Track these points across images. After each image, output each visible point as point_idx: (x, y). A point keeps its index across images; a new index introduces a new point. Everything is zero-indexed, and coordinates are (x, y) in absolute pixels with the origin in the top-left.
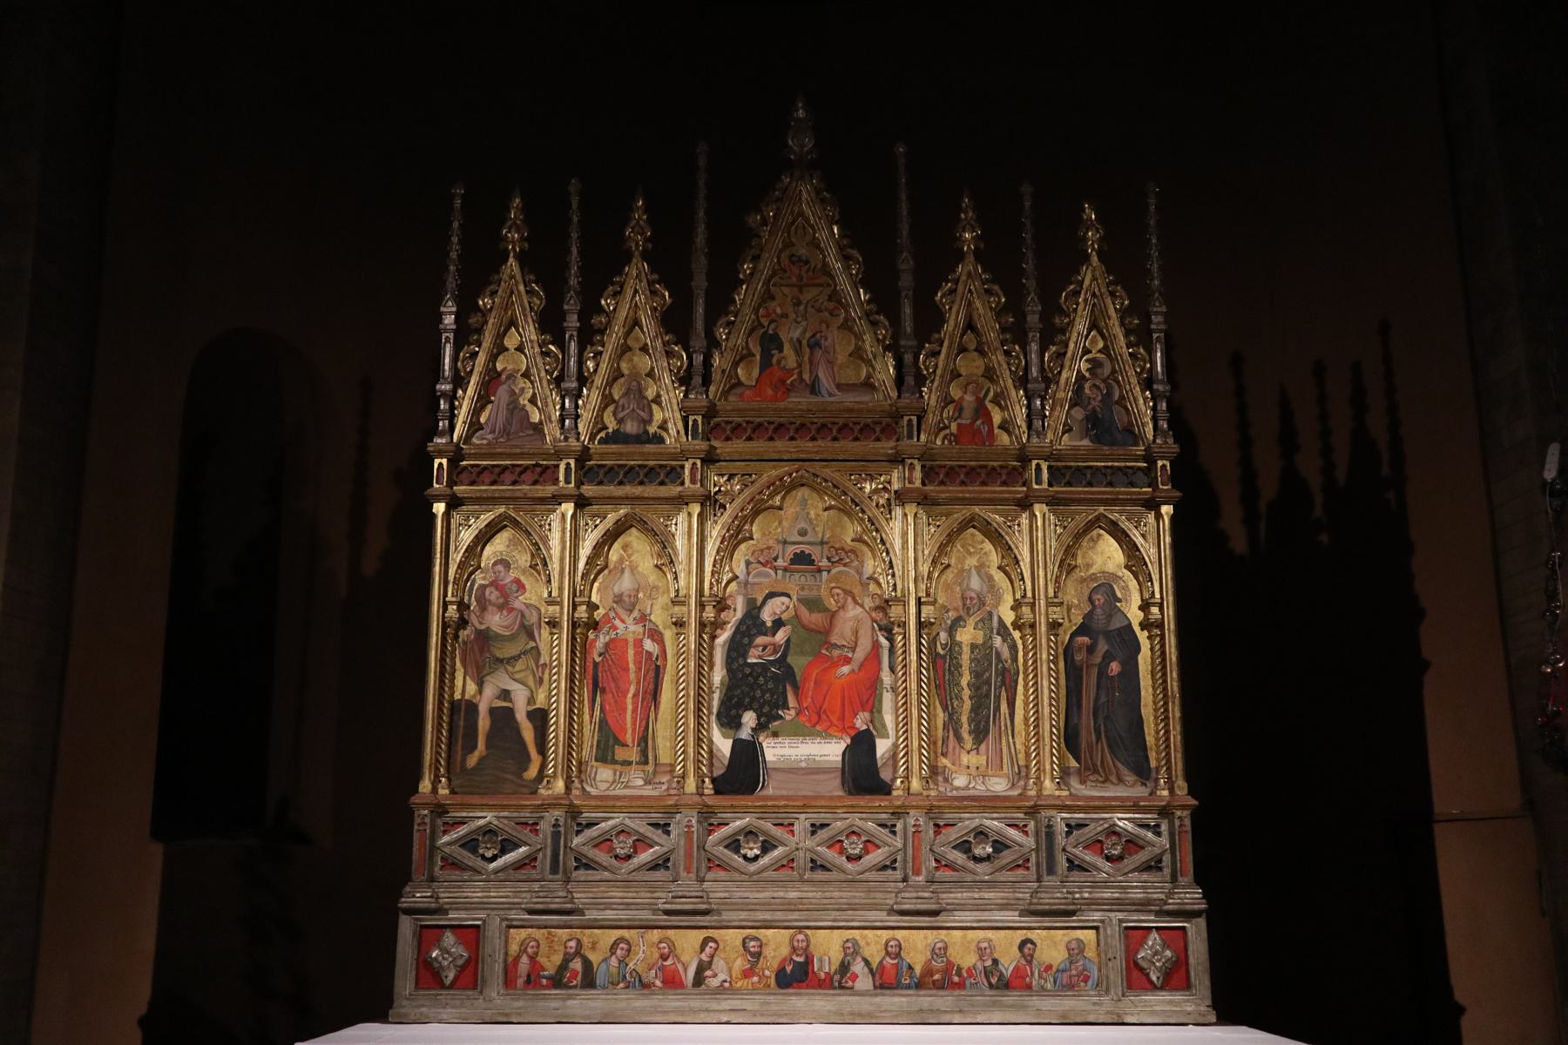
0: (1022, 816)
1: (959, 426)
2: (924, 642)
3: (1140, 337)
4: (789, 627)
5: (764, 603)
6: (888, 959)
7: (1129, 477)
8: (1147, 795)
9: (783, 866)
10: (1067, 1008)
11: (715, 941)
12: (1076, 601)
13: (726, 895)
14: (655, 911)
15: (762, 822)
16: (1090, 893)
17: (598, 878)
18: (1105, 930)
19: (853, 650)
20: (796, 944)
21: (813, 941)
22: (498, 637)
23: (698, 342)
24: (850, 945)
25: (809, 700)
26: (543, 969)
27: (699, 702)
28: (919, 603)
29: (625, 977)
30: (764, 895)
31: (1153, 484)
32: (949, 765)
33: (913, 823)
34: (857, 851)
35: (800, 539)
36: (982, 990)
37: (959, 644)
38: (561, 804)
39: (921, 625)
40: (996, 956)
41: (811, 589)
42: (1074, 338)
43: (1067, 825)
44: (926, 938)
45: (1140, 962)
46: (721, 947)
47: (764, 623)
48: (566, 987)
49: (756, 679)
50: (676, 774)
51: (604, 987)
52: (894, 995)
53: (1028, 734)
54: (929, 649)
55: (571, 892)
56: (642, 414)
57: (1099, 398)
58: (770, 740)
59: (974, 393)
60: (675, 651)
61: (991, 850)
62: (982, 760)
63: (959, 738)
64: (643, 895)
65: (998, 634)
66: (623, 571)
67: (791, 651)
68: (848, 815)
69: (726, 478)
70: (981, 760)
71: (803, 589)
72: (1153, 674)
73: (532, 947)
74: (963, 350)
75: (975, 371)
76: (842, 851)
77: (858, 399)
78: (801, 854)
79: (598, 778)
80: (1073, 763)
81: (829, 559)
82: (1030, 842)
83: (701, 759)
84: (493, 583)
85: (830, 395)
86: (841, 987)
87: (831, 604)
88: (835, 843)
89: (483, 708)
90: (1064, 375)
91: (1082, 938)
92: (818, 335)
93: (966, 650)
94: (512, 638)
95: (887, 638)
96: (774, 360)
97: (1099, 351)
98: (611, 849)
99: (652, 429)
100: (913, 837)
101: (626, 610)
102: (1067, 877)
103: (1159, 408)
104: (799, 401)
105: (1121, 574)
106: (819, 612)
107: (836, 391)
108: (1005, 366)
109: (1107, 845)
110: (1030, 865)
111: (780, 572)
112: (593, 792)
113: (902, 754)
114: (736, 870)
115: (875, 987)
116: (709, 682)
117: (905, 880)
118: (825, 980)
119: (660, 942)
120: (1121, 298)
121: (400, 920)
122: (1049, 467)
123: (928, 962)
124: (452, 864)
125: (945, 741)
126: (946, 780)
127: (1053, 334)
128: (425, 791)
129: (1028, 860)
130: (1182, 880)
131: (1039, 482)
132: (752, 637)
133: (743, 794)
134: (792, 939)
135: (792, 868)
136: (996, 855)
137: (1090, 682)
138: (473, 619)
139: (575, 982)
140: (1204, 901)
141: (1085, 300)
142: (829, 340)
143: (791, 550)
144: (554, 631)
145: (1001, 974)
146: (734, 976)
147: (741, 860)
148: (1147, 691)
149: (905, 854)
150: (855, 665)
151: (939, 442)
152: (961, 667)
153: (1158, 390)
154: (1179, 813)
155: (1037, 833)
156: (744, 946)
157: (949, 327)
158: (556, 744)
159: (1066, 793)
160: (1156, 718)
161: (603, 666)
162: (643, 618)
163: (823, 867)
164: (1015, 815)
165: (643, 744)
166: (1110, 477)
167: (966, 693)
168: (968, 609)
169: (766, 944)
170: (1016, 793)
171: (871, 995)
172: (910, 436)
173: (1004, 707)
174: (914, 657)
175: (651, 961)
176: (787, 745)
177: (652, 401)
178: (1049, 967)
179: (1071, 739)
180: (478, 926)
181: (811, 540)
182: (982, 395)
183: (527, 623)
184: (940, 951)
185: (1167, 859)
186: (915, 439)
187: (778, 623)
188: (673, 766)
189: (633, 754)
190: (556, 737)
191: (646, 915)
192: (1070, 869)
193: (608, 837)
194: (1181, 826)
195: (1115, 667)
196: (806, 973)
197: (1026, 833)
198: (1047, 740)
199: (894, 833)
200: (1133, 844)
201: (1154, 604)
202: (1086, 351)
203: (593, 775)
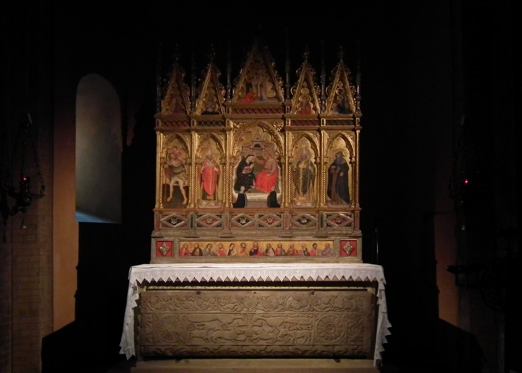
0: (315, 213)
1: (301, 109)
2: (290, 168)
3: (353, 82)
6: (279, 249)
7: (348, 122)
12: (332, 156)
13: (236, 233)
14: (218, 237)
15: (246, 215)
17: (203, 229)
18: (335, 241)
19: (271, 170)
20: (255, 245)
22: (175, 167)
23: (229, 86)
26: (189, 251)
28: (289, 157)
29: (210, 253)
30: (247, 232)
32: (296, 200)
34: (271, 222)
35: (257, 140)
39: (290, 164)
40: (307, 248)
43: (327, 215)
45: (344, 249)
47: (247, 163)
49: (245, 178)
50: (223, 203)
51: (205, 256)
53: (317, 192)
56: (213, 106)
57: (341, 100)
58: (248, 194)
59: (306, 100)
62: (305, 198)
63: (299, 193)
65: (310, 165)
66: (208, 149)
67: (254, 170)
68: (269, 213)
70: (305, 198)
71: (257, 154)
72: (352, 175)
74: (303, 87)
76: (267, 222)
78: (256, 223)
79: (202, 204)
80: (329, 199)
81: (265, 146)
82: (317, 219)
84: (173, 153)
85: (266, 100)
86: (266, 255)
87: (265, 158)
89: (171, 186)
90: (332, 94)
93: (301, 170)
94: (178, 167)
95: (280, 167)
96: (250, 90)
97: (342, 87)
98: (206, 222)
99: (216, 110)
104: (258, 102)
105: (345, 149)
107: (267, 99)
110: (316, 225)
111: (251, 149)
112: (201, 207)
114: (239, 227)
115: (275, 255)
116: (232, 178)
117: (283, 229)
119: (219, 245)
122: (326, 120)
123: (289, 249)
124: (165, 225)
125: (295, 194)
126: (295, 204)
127: (329, 83)
129: (316, 224)
130: (356, 229)
131: (323, 124)
132: (244, 167)
135: (254, 226)
137: (335, 178)
138: (168, 162)
141: (338, 73)
143: (255, 143)
146: (238, 252)
147: (240, 224)
149: (284, 222)
151: (295, 113)
152: (300, 174)
154: (356, 212)
155: (319, 217)
157: (299, 81)
158: (191, 195)
159: (327, 207)
162: (214, 162)
163: (262, 226)
166: (342, 122)
167: (301, 181)
168: (302, 159)
170: (313, 207)
172: (288, 112)
173: (311, 185)
174: (287, 172)
179: (329, 193)
180: (172, 241)
181: (260, 140)
183: (182, 164)
185: (353, 223)
186: (289, 113)
187: (251, 163)
188: (222, 201)
189: (212, 198)
190: (191, 193)
191: (216, 238)
193: (205, 219)
195: (342, 174)
196: (257, 252)
197: (316, 217)
199: (281, 217)
200: (344, 219)
201: (353, 157)
202: (338, 87)
203: (201, 203)
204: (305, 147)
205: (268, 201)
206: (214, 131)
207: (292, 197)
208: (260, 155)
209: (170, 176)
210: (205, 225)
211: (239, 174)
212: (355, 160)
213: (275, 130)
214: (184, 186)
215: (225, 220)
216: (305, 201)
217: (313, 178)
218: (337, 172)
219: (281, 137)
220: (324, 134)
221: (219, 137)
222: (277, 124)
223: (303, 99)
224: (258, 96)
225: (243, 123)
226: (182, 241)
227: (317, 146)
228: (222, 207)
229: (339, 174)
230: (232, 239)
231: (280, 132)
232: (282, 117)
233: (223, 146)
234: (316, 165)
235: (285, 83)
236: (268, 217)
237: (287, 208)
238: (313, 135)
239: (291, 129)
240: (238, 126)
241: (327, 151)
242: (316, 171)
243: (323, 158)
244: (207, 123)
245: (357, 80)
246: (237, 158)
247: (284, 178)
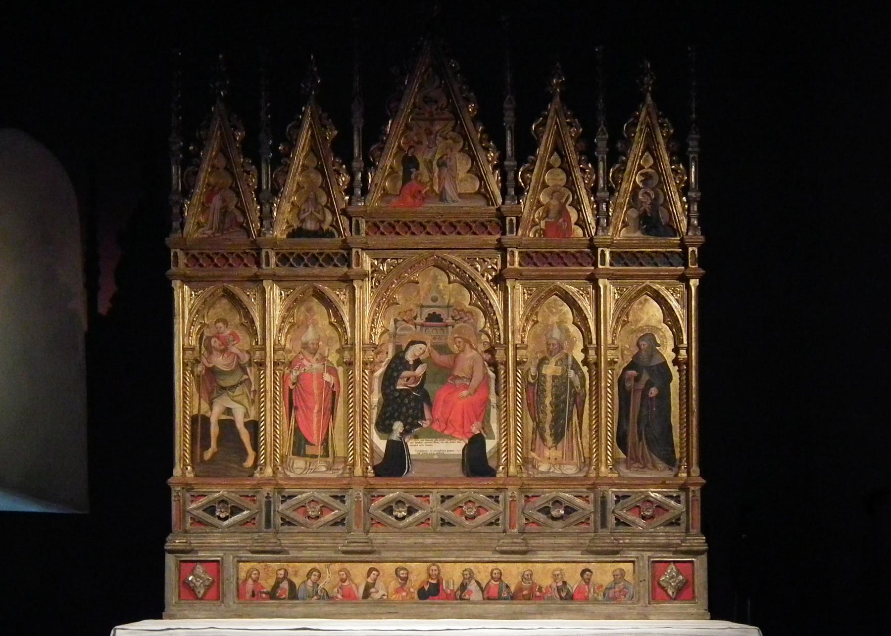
0: (585, 490)
3: (680, 156)
4: (424, 364)
5: (407, 348)
6: (493, 582)
7: (667, 258)
8: (672, 476)
9: (422, 523)
10: (611, 611)
11: (377, 570)
12: (628, 346)
13: (384, 541)
14: (336, 552)
15: (407, 494)
16: (630, 540)
18: (639, 563)
19: (470, 380)
20: (431, 572)
21: (442, 570)
22: (222, 373)
23: (357, 164)
24: (467, 572)
25: (439, 414)
26: (263, 588)
27: (363, 415)
28: (516, 348)
29: (317, 592)
30: (411, 541)
31: (686, 265)
32: (536, 457)
33: (510, 495)
37: (544, 376)
38: (270, 484)
39: (518, 364)
40: (565, 579)
41: (440, 338)
42: (631, 158)
43: (616, 496)
44: (518, 568)
45: (661, 582)
46: (381, 574)
47: (408, 362)
48: (279, 599)
49: (402, 401)
50: (348, 463)
51: (303, 599)
52: (496, 604)
53: (591, 436)
54: (523, 379)
55: (279, 540)
56: (318, 216)
57: (649, 202)
58: (412, 441)
59: (559, 200)
60: (346, 381)
61: (563, 512)
63: (543, 439)
64: (328, 541)
66: (307, 327)
68: (466, 490)
69: (380, 260)
70: (559, 453)
71: (435, 338)
72: (680, 395)
73: (255, 574)
74: (550, 167)
75: (560, 183)
76: (463, 513)
77: (473, 205)
78: (434, 515)
79: (295, 466)
80: (623, 456)
81: (453, 318)
82: (590, 507)
83: (365, 453)
85: (454, 201)
86: (461, 599)
87: (455, 348)
88: (457, 507)
89: (213, 421)
90: (624, 185)
92: (445, 157)
93: (549, 379)
94: (232, 372)
95: (494, 372)
96: (413, 176)
97: (650, 167)
98: (306, 512)
99: (326, 227)
100: (510, 504)
101: (311, 353)
102: (614, 529)
103: (692, 209)
104: (432, 206)
105: (661, 327)
106: (447, 354)
107: (458, 198)
108: (581, 180)
109: (643, 507)
110: (590, 522)
111: (418, 327)
112: (292, 475)
113: (503, 450)
114: (390, 525)
115: (484, 599)
116: (369, 402)
117: (504, 531)
119: (340, 571)
120: (667, 127)
121: (166, 557)
122: (611, 252)
123: (519, 584)
126: (534, 467)
127: (615, 157)
128: (177, 475)
130: (693, 531)
131: (603, 263)
132: (399, 372)
133: (395, 476)
134: (428, 570)
135: (428, 524)
136: (566, 515)
138: (204, 360)
139: (284, 596)
140: (706, 544)
141: (641, 130)
142: (453, 161)
143: (426, 312)
144: (261, 368)
145: (568, 590)
146: (390, 591)
147: (393, 519)
148: (675, 407)
150: (471, 390)
151: (531, 235)
152: (545, 391)
153: (691, 196)
154: (692, 488)
155: (595, 501)
156: (396, 574)
157: (540, 151)
158: (265, 444)
159: (616, 475)
160: (681, 424)
161: (296, 392)
162: (323, 358)
163: (450, 524)
164: (580, 490)
165: (325, 444)
166: (652, 259)
167: (549, 409)
168: (551, 352)
170: (582, 475)
171: (481, 604)
173: (575, 418)
174: (511, 385)
176: (424, 444)
177: (326, 206)
178: (601, 586)
179: (621, 441)
180: (217, 561)
181: (441, 304)
182: (563, 200)
183: (241, 363)
185: (683, 518)
187: (418, 362)
188: (346, 459)
189: (319, 451)
190: (265, 439)
192: (617, 524)
193: (304, 504)
194: (693, 496)
195: (653, 391)
196: (438, 591)
197: (588, 501)
198: (603, 441)
199: (498, 502)
200: (660, 508)
201: (682, 348)
202: (641, 167)
203: (291, 465)
204: (557, 323)
205: (463, 460)
206: (322, 279)
207: (527, 449)
208: (442, 342)
209: (210, 393)
210: (301, 521)
211: (388, 391)
212: (686, 357)
213: (480, 277)
214: (246, 420)
215: (354, 507)
216: (559, 460)
217: (578, 400)
218: (641, 386)
219: (494, 297)
220: (605, 287)
221: (334, 296)
222: (485, 261)
223: (552, 199)
224: (433, 191)
225: (397, 259)
226: (244, 562)
227: (589, 320)
228: (347, 475)
229: (645, 391)
230: (371, 556)
231: (492, 284)
232: (496, 245)
233: (346, 319)
234: (585, 367)
235: (502, 157)
236: (464, 502)
237: (514, 479)
238: (578, 292)
239: (521, 275)
240: (384, 268)
241: (614, 333)
242: (588, 382)
243: (606, 350)
244: (303, 259)
245: (690, 149)
246: (383, 348)
247: (506, 401)
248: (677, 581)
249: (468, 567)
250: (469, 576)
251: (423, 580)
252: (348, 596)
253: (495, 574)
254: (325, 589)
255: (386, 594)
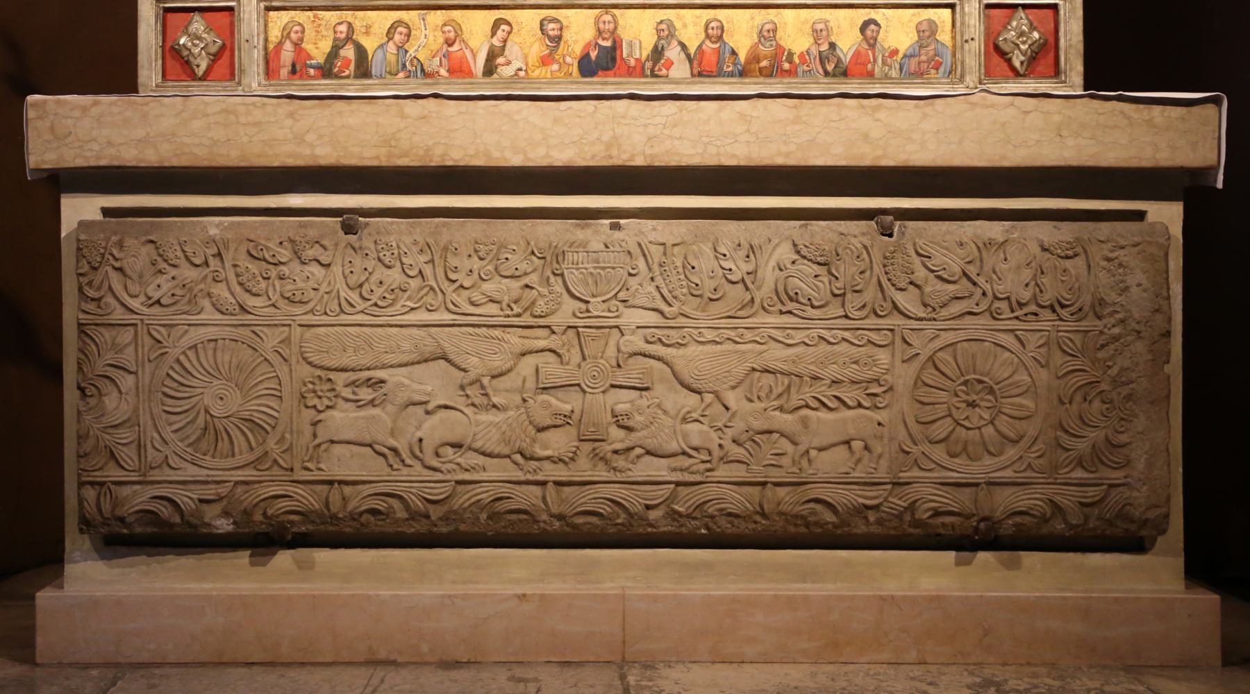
6: (708, 43)
11: (509, 24)
20: (601, 25)
21: (621, 22)
24: (664, 26)
26: (310, 58)
29: (404, 65)
36: (817, 77)
40: (833, 39)
45: (1001, 44)
46: (515, 30)
48: (337, 76)
73: (297, 32)
86: (653, 75)
91: (934, 18)
115: (693, 75)
118: (634, 68)
119: (445, 25)
123: (755, 47)
134: (597, 20)
139: (347, 72)
145: (839, 60)
156: (542, 29)
169: (567, 27)
175: (435, 47)
178: (895, 52)
184: (767, 34)
196: (614, 59)
248: (1030, 42)
249: (665, 18)
250: (666, 33)
251: (587, 41)
252: (459, 70)
253: (713, 29)
254: (418, 59)
255: (524, 68)
